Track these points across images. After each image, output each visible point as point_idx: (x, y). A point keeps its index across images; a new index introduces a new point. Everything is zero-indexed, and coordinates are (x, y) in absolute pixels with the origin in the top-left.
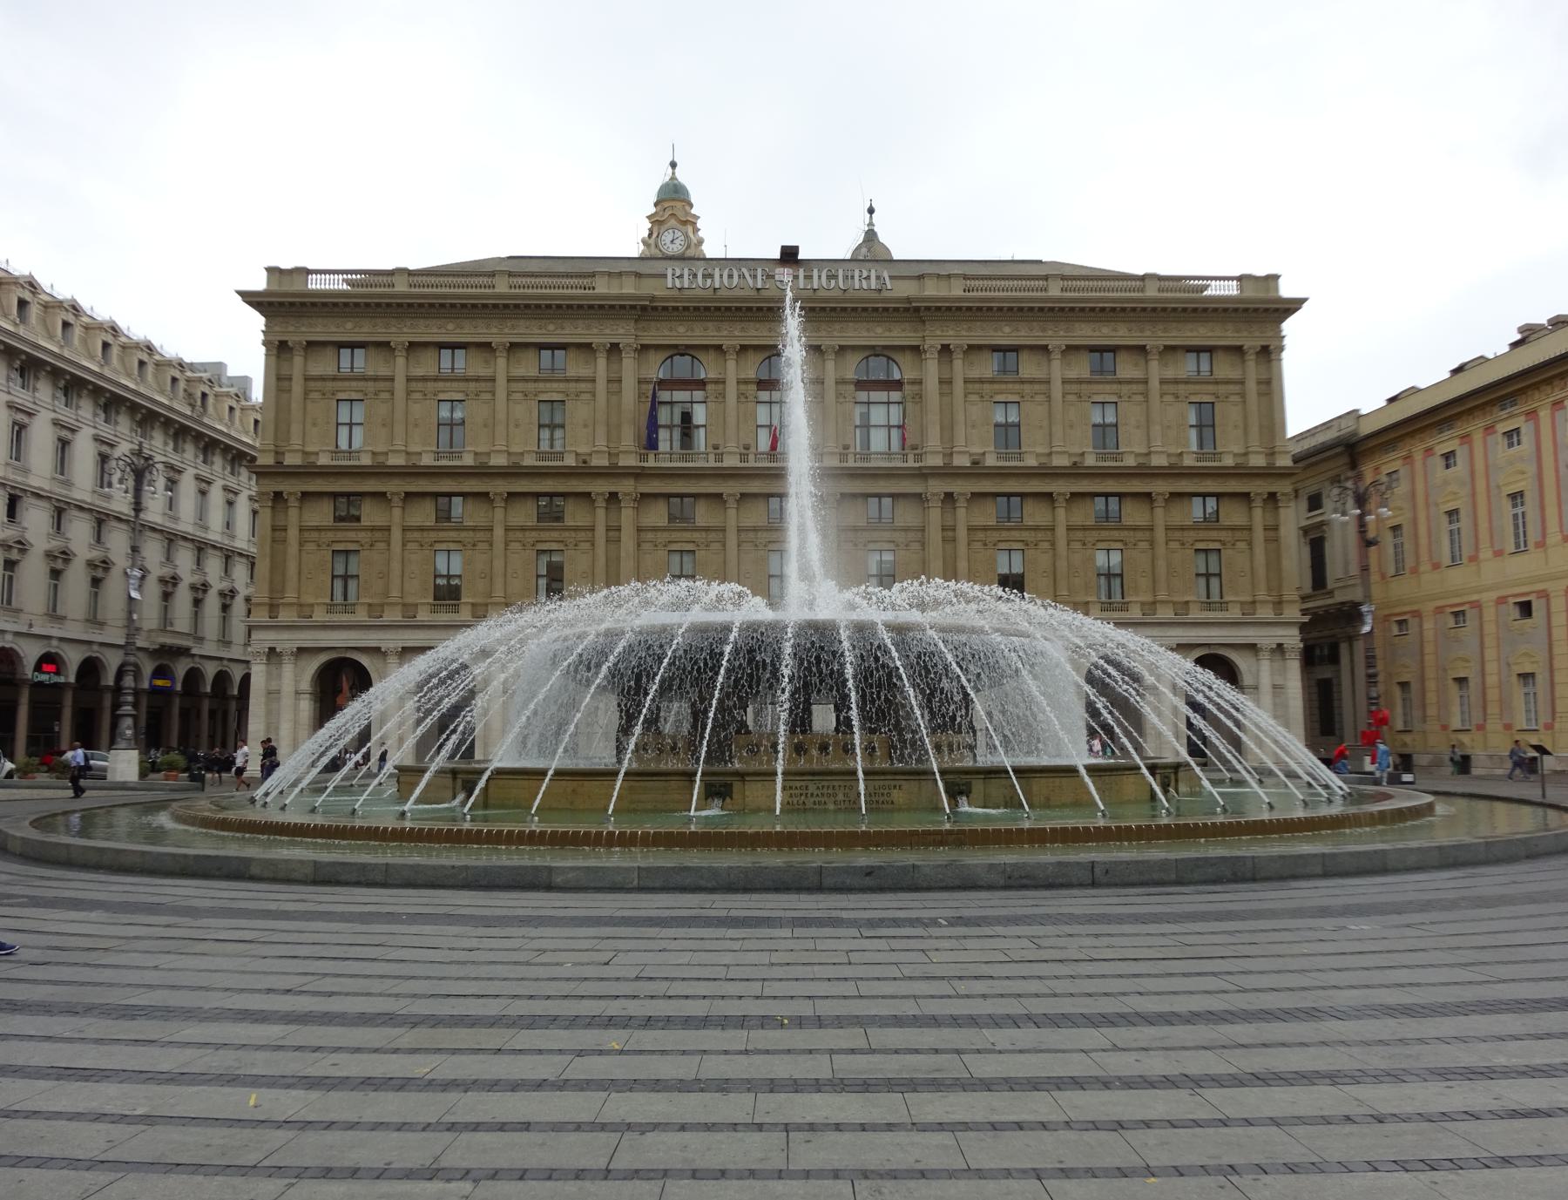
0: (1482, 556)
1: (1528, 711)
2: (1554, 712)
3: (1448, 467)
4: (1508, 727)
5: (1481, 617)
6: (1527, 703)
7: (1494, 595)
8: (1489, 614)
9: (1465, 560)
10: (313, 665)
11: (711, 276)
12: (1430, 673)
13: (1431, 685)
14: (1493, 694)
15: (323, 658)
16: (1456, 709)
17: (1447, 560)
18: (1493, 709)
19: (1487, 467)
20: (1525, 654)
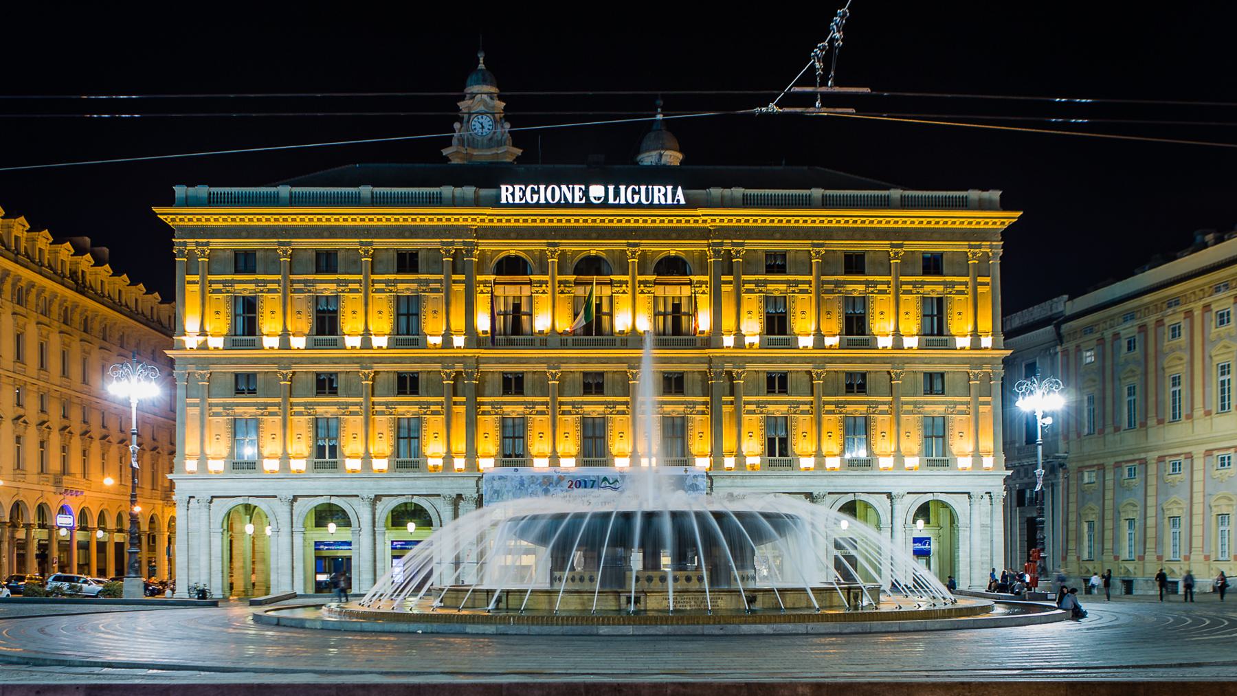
0: (1149, 423)
1: (1175, 545)
2: (1191, 548)
3: (1129, 349)
4: (1160, 558)
5: (1146, 472)
6: (1174, 539)
7: (1156, 454)
8: (1152, 469)
9: (1138, 426)
10: (221, 508)
11: (538, 192)
12: (1109, 514)
13: (1109, 524)
14: (1151, 533)
15: (232, 503)
16: (1126, 544)
17: (1125, 425)
18: (1150, 544)
19: (1156, 352)
20: (1175, 502)
